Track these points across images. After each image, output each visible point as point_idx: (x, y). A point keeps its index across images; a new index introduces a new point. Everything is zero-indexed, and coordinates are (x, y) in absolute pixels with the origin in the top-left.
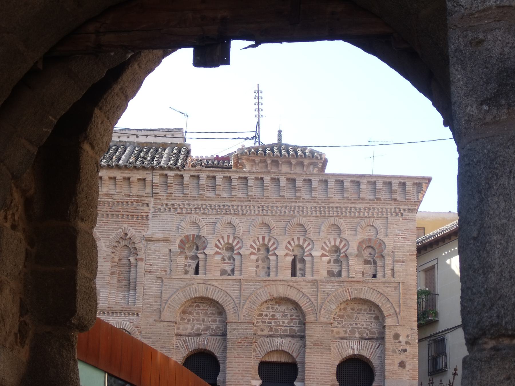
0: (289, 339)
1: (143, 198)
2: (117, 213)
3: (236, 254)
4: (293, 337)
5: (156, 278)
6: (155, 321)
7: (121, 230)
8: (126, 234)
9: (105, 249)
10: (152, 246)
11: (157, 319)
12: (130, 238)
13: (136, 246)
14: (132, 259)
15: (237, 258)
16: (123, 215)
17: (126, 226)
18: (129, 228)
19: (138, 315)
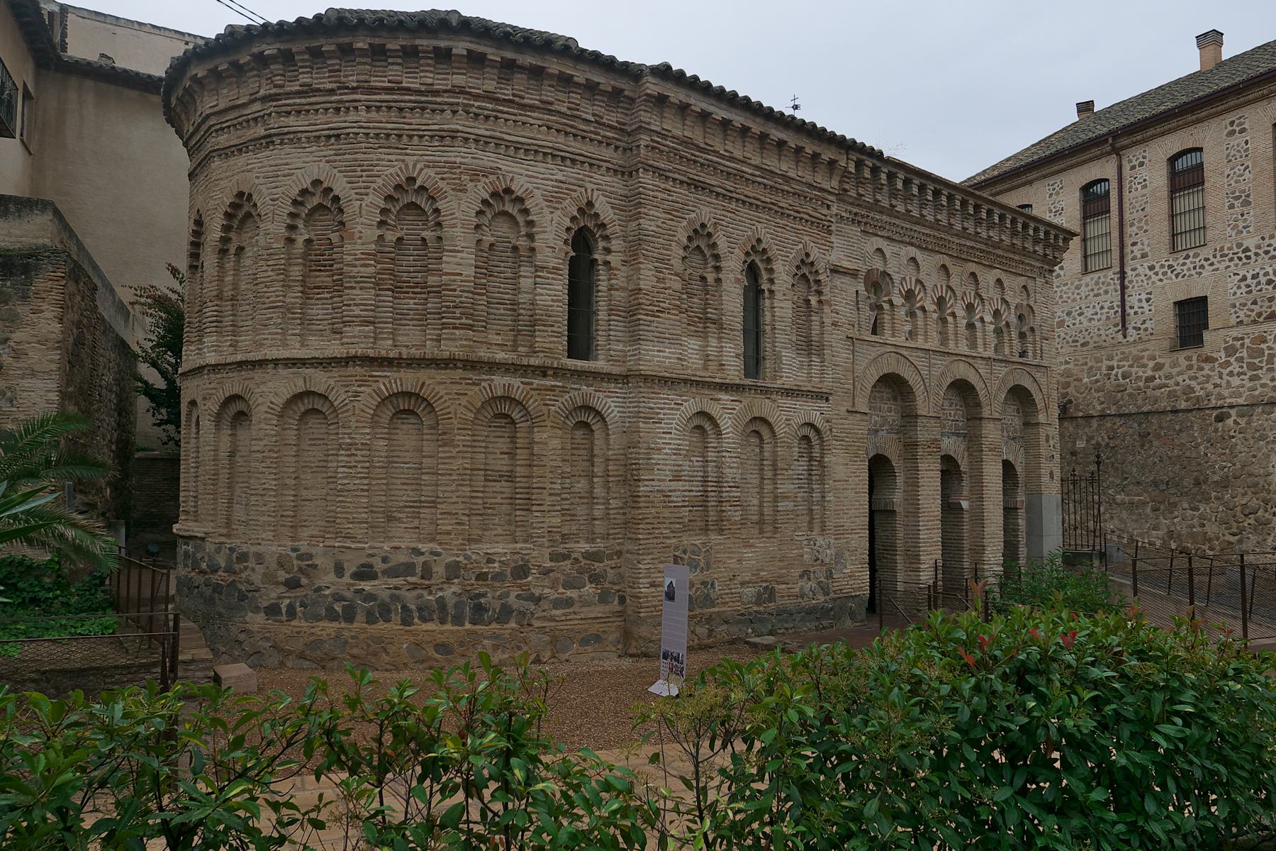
0: (954, 438)
1: (826, 195)
2: (797, 215)
3: (918, 308)
4: (958, 435)
5: (844, 338)
6: (848, 411)
7: (801, 246)
8: (807, 255)
9: (785, 277)
10: (839, 281)
11: (850, 409)
12: (812, 264)
13: (821, 277)
14: (813, 300)
15: (919, 313)
16: (801, 219)
17: (807, 238)
18: (812, 244)
19: (827, 400)
